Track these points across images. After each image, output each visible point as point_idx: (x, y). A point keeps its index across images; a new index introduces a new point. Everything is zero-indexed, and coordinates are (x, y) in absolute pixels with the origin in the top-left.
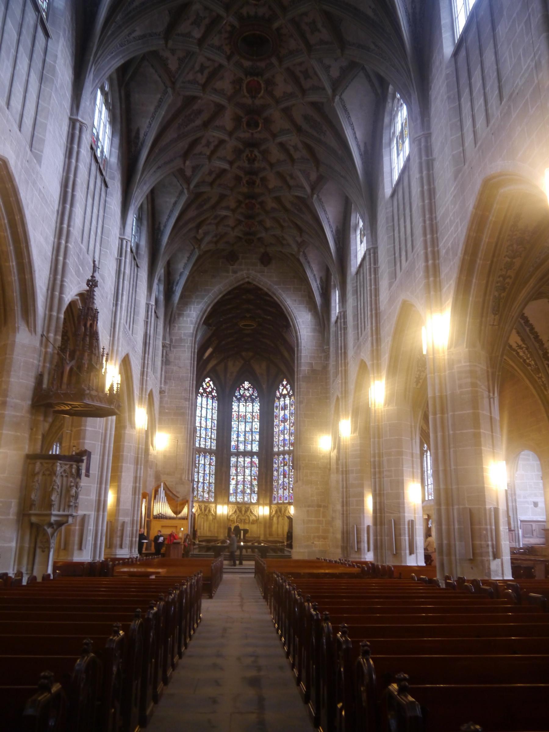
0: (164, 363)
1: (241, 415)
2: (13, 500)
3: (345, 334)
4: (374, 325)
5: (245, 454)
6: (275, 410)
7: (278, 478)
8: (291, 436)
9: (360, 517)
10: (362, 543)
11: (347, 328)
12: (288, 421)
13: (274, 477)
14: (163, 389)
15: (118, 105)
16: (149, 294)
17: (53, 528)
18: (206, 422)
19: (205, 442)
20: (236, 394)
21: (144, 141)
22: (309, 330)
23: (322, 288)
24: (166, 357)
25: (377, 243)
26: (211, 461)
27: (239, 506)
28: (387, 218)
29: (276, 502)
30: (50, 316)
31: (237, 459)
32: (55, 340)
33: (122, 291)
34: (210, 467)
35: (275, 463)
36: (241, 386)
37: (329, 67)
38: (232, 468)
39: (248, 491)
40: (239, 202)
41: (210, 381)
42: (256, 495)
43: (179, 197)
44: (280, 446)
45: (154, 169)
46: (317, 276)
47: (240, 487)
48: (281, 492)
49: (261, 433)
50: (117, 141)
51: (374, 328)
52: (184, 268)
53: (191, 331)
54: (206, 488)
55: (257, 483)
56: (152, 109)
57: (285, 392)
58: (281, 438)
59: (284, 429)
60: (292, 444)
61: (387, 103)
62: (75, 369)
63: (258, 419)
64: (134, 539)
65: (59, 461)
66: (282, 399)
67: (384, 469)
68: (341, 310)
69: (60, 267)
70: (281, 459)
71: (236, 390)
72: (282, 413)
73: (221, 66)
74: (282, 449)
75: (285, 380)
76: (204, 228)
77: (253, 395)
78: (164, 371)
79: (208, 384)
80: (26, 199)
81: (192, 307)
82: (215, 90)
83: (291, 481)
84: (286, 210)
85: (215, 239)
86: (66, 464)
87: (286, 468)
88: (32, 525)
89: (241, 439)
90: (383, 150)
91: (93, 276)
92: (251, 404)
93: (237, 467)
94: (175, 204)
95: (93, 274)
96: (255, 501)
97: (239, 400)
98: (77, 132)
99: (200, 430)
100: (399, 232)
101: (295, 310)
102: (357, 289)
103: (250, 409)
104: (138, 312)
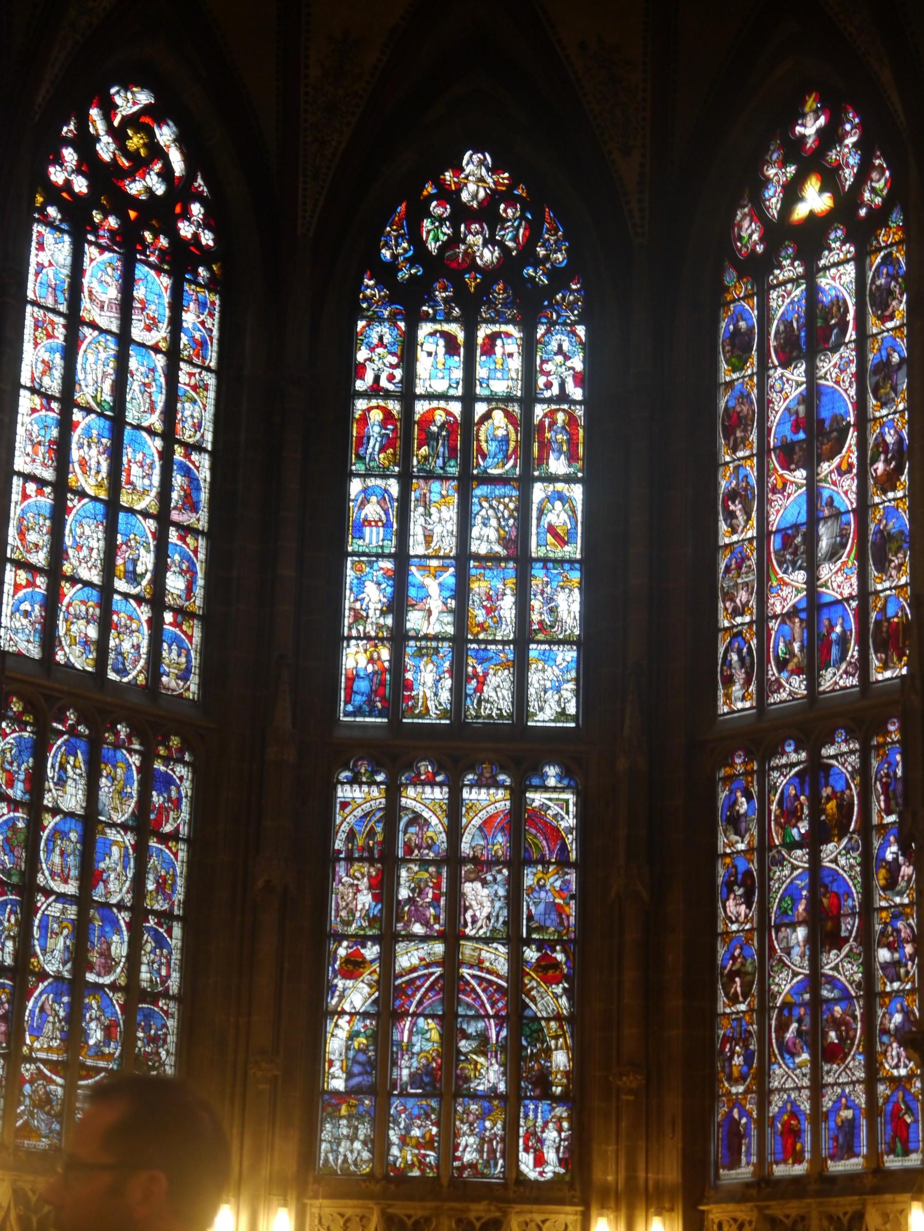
1: (428, 418)
6: (726, 374)
7: (766, 952)
8: (882, 566)
12: (852, 438)
13: (721, 951)
18: (115, 453)
19: (105, 624)
20: (386, 254)
26: (157, 799)
27: (400, 1209)
29: (745, 1172)
31: (393, 792)
34: (141, 852)
35: (735, 822)
36: (430, 189)
38: (341, 869)
42: (561, 1111)
44: (773, 670)
54: (96, 1035)
63: (572, 458)
66: (790, 269)
71: (386, 217)
75: (811, 103)
77: (527, 254)
79: (135, 142)
83: (893, 970)
96: (552, 1168)
99: (59, 514)
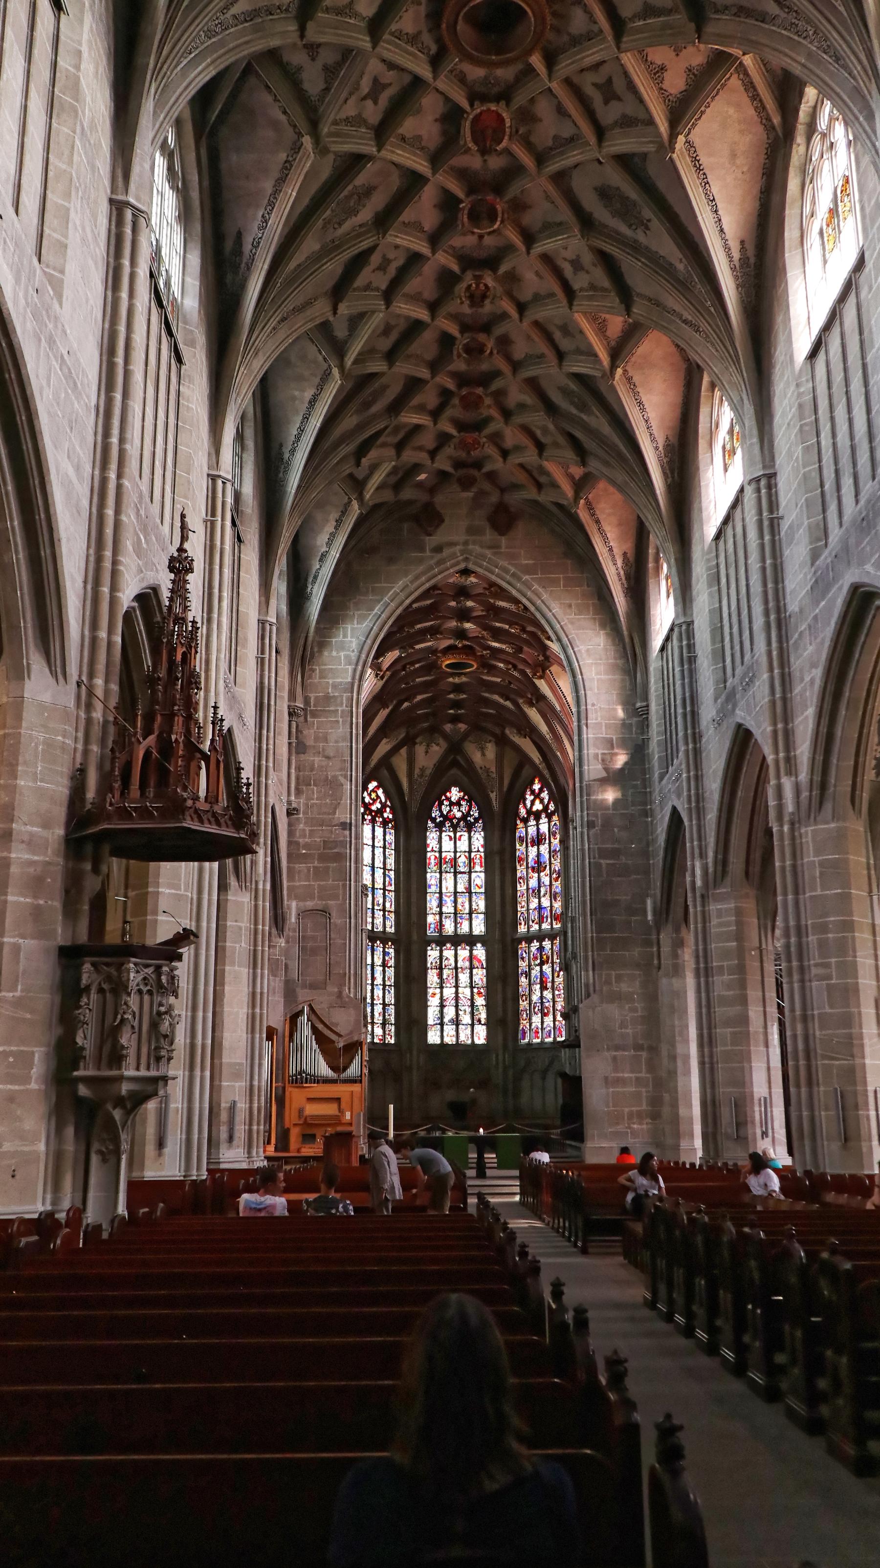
0: (294, 750)
2: (35, 1049)
3: (692, 672)
4: (774, 645)
5: (457, 940)
6: (518, 847)
7: (530, 990)
9: (742, 1069)
10: (749, 1126)
11: (695, 657)
14: (294, 805)
15: (194, 178)
16: (263, 599)
17: (124, 1107)
19: (373, 918)
21: (252, 259)
22: (602, 668)
23: (628, 577)
24: (297, 738)
25: (774, 466)
28: (800, 406)
30: (94, 640)
31: (441, 952)
32: (107, 692)
33: (220, 591)
34: (384, 971)
35: (523, 959)
37: (663, 69)
39: (466, 1019)
40: (446, 395)
41: (377, 787)
43: (320, 388)
45: (273, 323)
46: (615, 550)
47: (450, 1012)
48: (536, 1019)
49: (489, 895)
50: (195, 259)
51: (775, 653)
52: (329, 544)
53: (349, 680)
55: (484, 1003)
56: (268, 186)
57: (538, 806)
58: (534, 904)
59: (539, 887)
60: (556, 918)
61: (794, 146)
62: (155, 754)
64: (255, 1127)
65: (133, 960)
66: (532, 822)
67: (812, 962)
68: (682, 620)
69: (109, 531)
70: (533, 949)
72: (533, 852)
73: (417, 82)
74: (535, 927)
76: (373, 454)
77: (468, 813)
78: (293, 766)
79: (373, 795)
80: (37, 376)
81: (349, 626)
82: (403, 139)
84: (551, 408)
85: (393, 479)
86: (147, 966)
87: (547, 968)
88: (80, 1101)
89: (448, 908)
90: (787, 255)
91: (181, 550)
92: (466, 834)
93: (441, 968)
94: (313, 402)
95: (182, 543)
97: (440, 827)
98: (128, 230)
100: (834, 435)
101: (570, 626)
102: (718, 572)
103: (463, 845)
104: (246, 639)
